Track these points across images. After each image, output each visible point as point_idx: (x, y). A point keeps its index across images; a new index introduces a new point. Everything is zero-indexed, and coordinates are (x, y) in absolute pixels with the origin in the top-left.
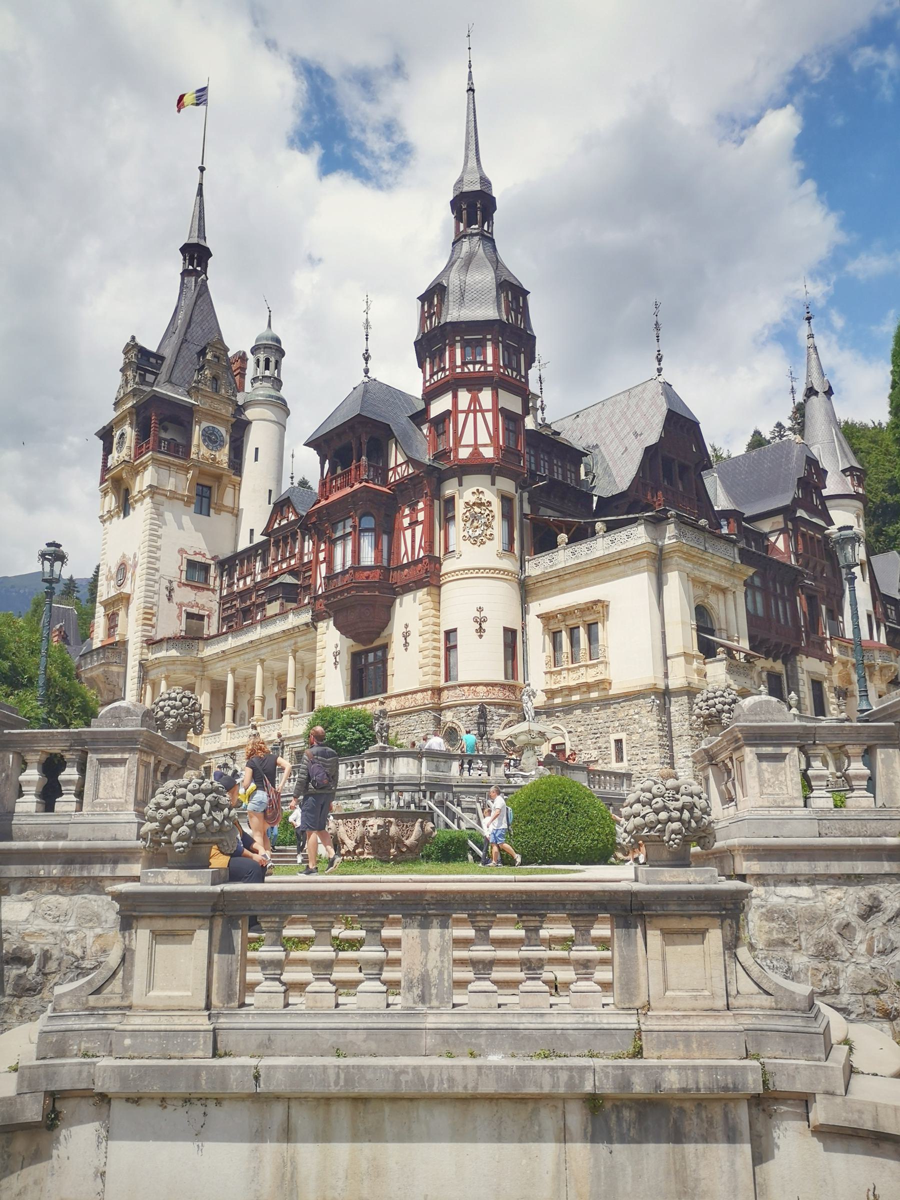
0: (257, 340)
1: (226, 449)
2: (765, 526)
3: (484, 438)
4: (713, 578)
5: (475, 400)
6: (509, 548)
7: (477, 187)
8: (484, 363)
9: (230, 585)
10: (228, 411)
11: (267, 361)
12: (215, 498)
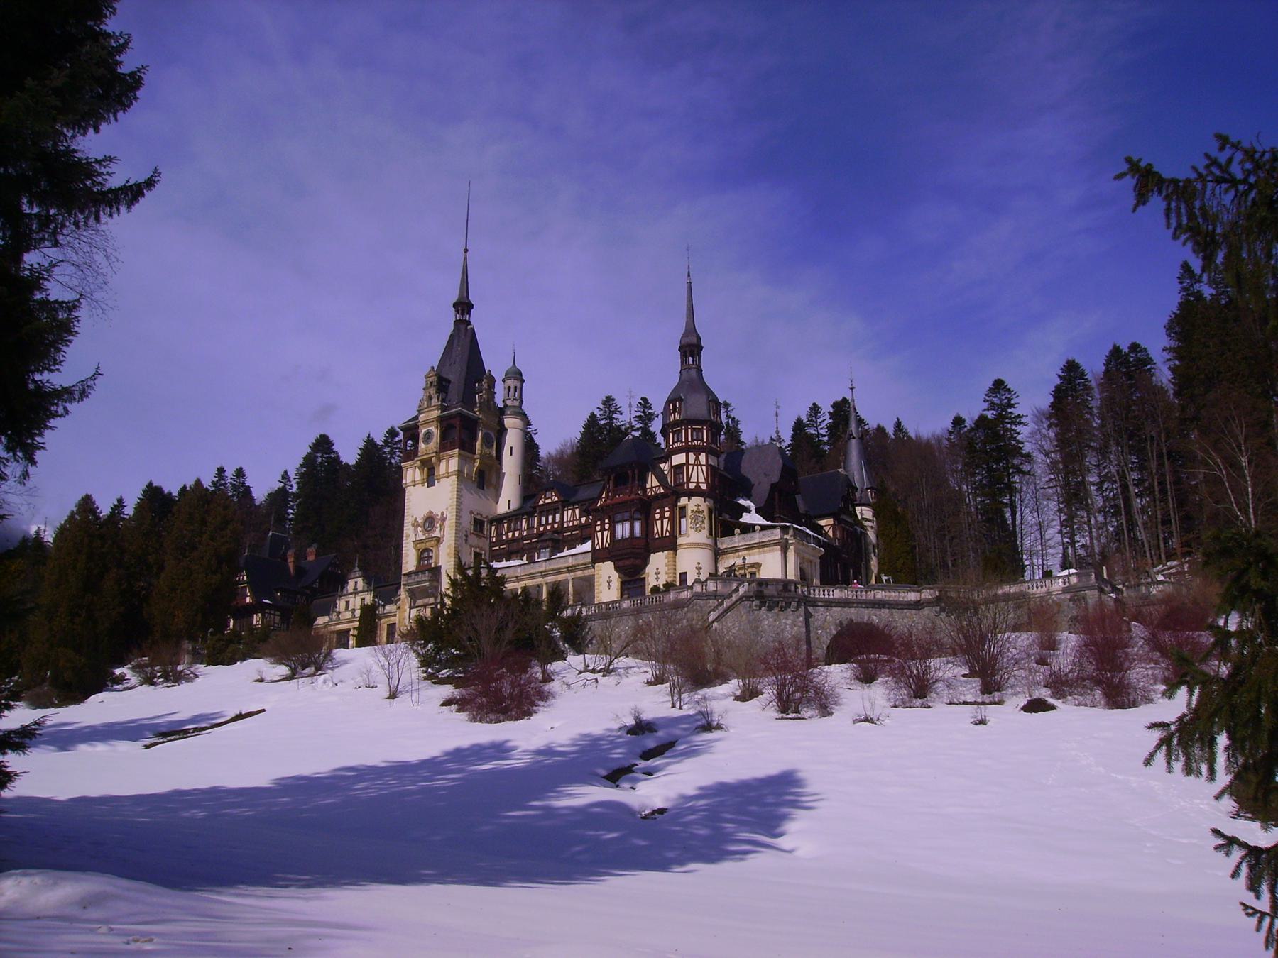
2: (822, 523)
3: (702, 479)
5: (697, 459)
6: (711, 534)
7: (694, 340)
9: (499, 534)
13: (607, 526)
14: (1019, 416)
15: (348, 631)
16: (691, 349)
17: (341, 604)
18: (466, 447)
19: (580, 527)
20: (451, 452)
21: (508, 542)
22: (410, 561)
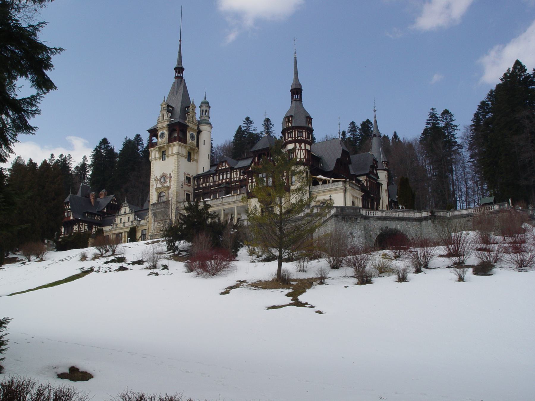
0: (202, 103)
1: (196, 140)
2: (361, 178)
3: (302, 157)
4: (355, 195)
5: (300, 146)
8: (303, 137)
9: (198, 185)
10: (196, 128)
11: (206, 110)
12: (192, 156)
13: (254, 180)
14: (456, 126)
15: (122, 233)
16: (297, 91)
17: (118, 220)
18: (183, 140)
19: (240, 181)
20: (174, 143)
21: (203, 188)
22: (153, 197)
